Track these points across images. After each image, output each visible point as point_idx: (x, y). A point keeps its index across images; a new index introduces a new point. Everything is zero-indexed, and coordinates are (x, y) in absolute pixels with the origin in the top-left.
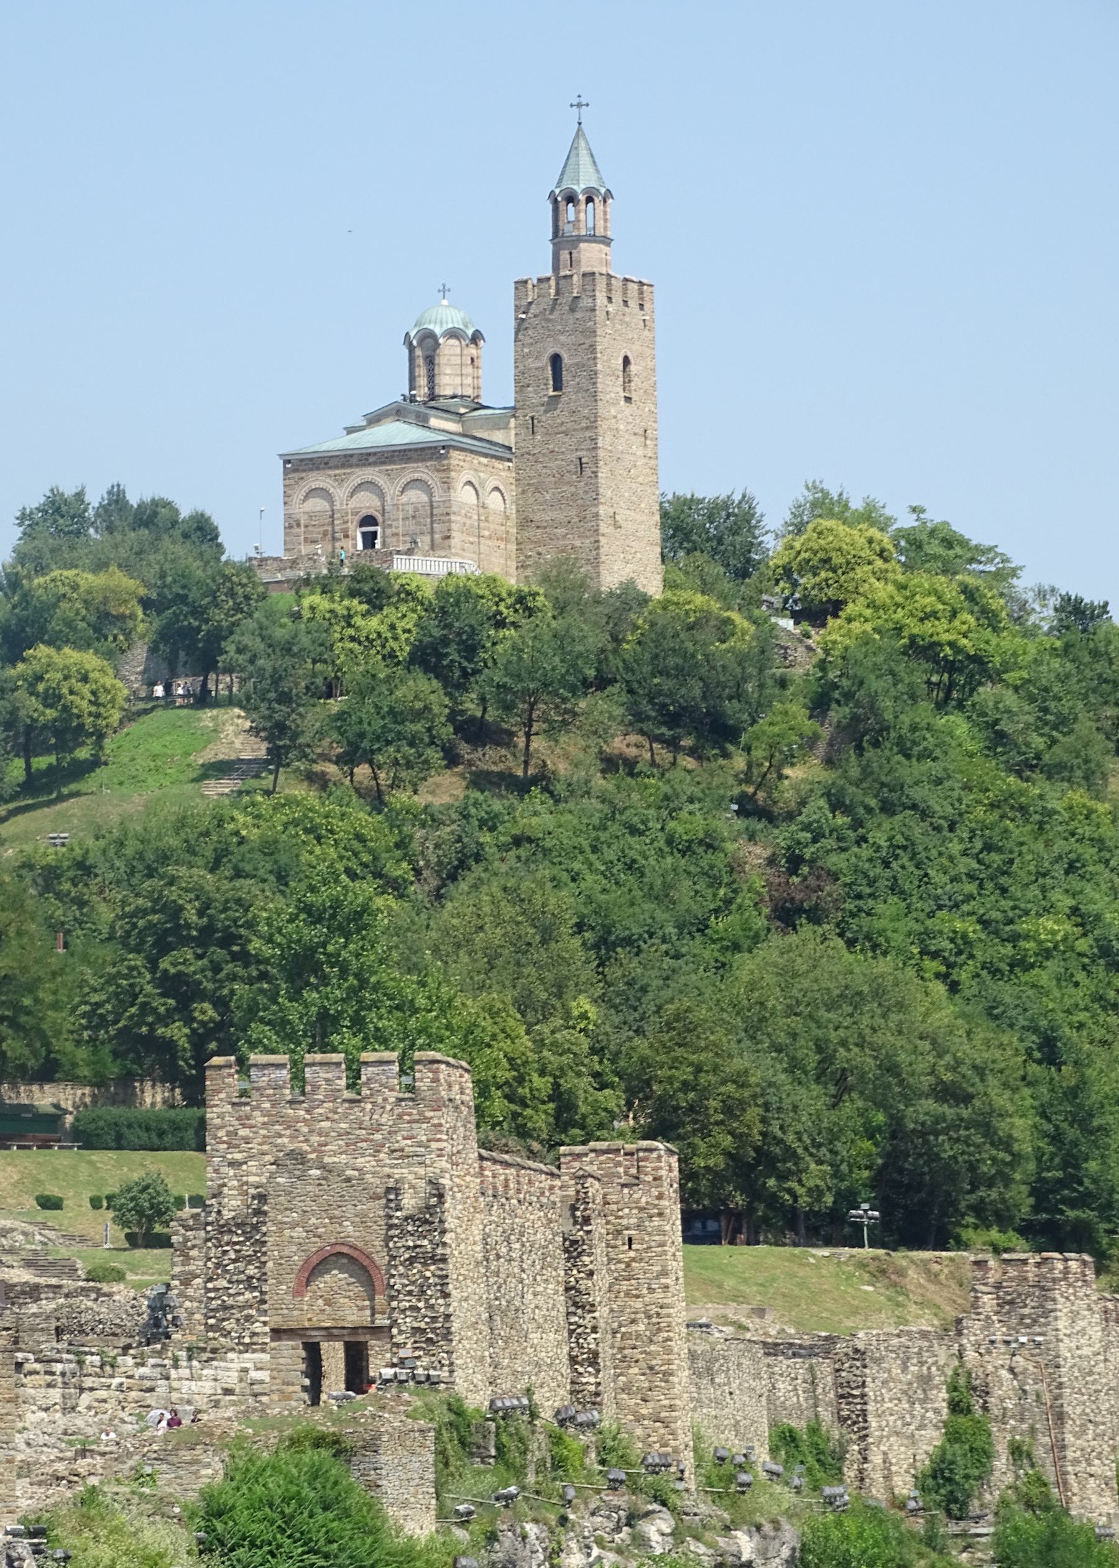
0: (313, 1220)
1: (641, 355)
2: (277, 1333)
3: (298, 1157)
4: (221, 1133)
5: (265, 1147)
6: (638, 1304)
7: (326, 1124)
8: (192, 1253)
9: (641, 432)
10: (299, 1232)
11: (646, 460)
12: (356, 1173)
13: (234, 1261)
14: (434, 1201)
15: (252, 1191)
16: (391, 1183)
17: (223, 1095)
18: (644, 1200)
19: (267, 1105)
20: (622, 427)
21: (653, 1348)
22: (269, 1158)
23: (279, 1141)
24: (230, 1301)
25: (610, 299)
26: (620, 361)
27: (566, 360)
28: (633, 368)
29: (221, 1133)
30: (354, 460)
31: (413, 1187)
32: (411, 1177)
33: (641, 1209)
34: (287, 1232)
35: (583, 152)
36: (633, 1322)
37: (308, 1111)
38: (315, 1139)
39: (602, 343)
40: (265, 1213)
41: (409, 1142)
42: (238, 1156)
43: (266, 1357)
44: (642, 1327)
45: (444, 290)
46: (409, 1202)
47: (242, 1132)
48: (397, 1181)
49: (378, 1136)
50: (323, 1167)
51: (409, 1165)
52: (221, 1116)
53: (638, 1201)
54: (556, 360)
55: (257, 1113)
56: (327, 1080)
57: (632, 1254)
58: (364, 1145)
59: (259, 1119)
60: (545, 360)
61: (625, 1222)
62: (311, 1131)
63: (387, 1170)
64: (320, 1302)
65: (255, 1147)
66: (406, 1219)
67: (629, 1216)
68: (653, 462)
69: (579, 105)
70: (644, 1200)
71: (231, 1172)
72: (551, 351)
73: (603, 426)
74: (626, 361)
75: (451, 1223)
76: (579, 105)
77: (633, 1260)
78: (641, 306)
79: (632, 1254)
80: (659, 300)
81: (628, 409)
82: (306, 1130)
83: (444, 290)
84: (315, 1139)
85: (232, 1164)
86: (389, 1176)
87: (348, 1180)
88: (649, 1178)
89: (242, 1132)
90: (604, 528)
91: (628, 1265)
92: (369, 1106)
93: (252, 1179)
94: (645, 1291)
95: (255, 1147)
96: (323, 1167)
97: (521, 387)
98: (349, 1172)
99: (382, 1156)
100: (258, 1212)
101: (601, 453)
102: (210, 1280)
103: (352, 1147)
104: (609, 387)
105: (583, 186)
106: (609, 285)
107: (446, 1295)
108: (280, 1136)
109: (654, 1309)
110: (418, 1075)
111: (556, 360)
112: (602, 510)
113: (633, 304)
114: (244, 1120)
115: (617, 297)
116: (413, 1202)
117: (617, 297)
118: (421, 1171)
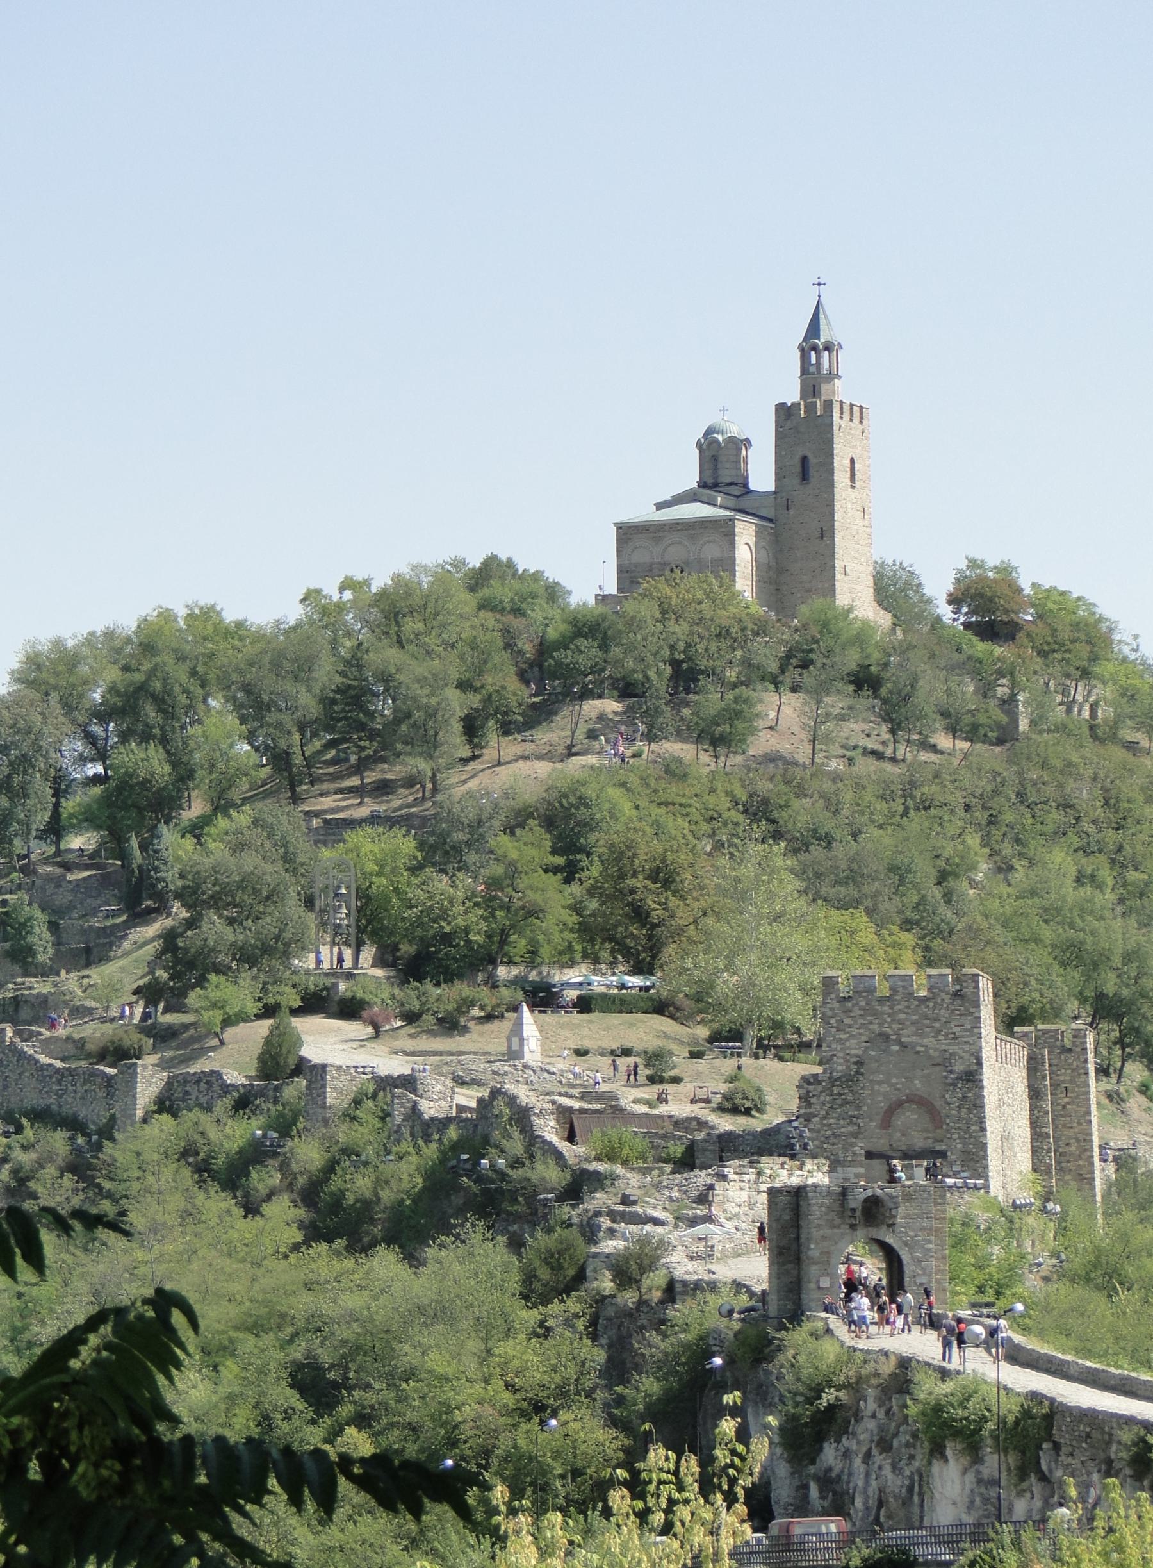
0: (894, 1080)
2: (870, 1155)
3: (885, 1037)
4: (833, 1021)
5: (862, 1031)
6: (1071, 1133)
7: (902, 1016)
8: (813, 1100)
10: (885, 1088)
12: (922, 1049)
13: (841, 1105)
14: (975, 1068)
15: (855, 1060)
16: (947, 1055)
17: (833, 996)
18: (1075, 1063)
19: (863, 1003)
20: (849, 506)
21: (1081, 1163)
22: (864, 1038)
23: (871, 1027)
24: (838, 1132)
25: (841, 418)
26: (848, 461)
27: (813, 460)
28: (857, 466)
29: (833, 1021)
30: (666, 528)
31: (961, 1058)
32: (960, 1052)
33: (1073, 1070)
34: (876, 1087)
35: (822, 316)
36: (1067, 1144)
37: (891, 1007)
38: (896, 1026)
39: (838, 447)
40: (862, 1074)
41: (958, 1029)
42: (843, 1036)
43: (862, 1170)
44: (1073, 1148)
46: (959, 1067)
47: (847, 1021)
48: (951, 1054)
49: (937, 1025)
50: (900, 1043)
51: (958, 1044)
52: (831, 1009)
53: (1072, 1064)
54: (804, 460)
55: (856, 1008)
56: (903, 987)
57: (1067, 1100)
58: (928, 1030)
59: (857, 1012)
61: (1062, 1078)
62: (893, 1021)
63: (944, 1047)
64: (899, 1134)
65: (854, 1031)
66: (957, 1079)
67: (1064, 1074)
68: (868, 530)
69: (819, 284)
70: (1075, 1063)
71: (839, 1047)
74: (852, 461)
75: (985, 1083)
76: (819, 284)
77: (1068, 1103)
78: (861, 422)
79: (1067, 1100)
80: (871, 415)
82: (889, 1020)
83: (724, 410)
84: (896, 1026)
85: (840, 1041)
86: (945, 1051)
87: (918, 1053)
88: (1078, 1049)
89: (847, 1021)
90: (838, 576)
91: (1064, 1107)
92: (931, 1005)
93: (853, 1052)
94: (1075, 1125)
95: (854, 1031)
96: (900, 1043)
97: (780, 476)
98: (919, 1049)
99: (941, 1038)
100: (858, 1073)
101: (836, 523)
102: (824, 1118)
103: (919, 1032)
104: (841, 478)
105: (822, 340)
106: (841, 408)
107: (983, 1130)
108: (871, 1023)
109: (1081, 1137)
110: (964, 984)
111: (804, 460)
112: (838, 564)
113: (856, 419)
114: (847, 1011)
115: (846, 416)
116: (961, 1068)
117: (846, 416)
118: (967, 1047)
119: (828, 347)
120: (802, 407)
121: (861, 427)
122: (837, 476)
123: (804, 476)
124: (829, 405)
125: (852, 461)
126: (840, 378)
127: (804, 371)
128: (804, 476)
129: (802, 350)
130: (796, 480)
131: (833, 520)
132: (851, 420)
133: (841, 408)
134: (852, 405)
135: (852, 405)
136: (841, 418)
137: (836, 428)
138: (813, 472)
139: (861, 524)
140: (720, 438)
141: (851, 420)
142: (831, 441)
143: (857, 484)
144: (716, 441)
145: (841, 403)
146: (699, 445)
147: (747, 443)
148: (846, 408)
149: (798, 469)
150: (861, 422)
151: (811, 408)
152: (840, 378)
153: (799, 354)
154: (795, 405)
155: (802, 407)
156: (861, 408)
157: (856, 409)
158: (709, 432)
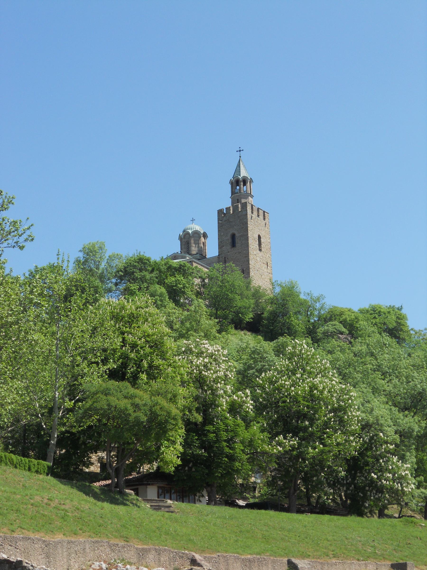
1: (264, 236)
9: (266, 263)
11: (268, 274)
20: (258, 259)
25: (252, 213)
27: (237, 235)
28: (262, 240)
35: (242, 166)
45: (193, 220)
54: (233, 236)
60: (229, 237)
68: (270, 275)
72: (231, 232)
73: (251, 257)
74: (259, 237)
76: (240, 151)
78: (264, 219)
81: (261, 254)
83: (193, 220)
104: (253, 244)
105: (241, 176)
106: (252, 208)
111: (233, 236)
113: (261, 217)
115: (255, 213)
119: (245, 181)
120: (231, 209)
121: (264, 222)
122: (251, 241)
123: (233, 244)
124: (244, 206)
125: (259, 237)
126: (252, 196)
127: (233, 193)
128: (233, 244)
129: (231, 183)
130: (229, 247)
131: (249, 264)
132: (258, 216)
133: (252, 208)
134: (258, 209)
135: (258, 209)
136: (252, 213)
137: (249, 217)
138: (237, 241)
139: (265, 270)
140: (190, 232)
141: (258, 216)
142: (247, 223)
143: (262, 249)
144: (188, 233)
145: (252, 206)
146: (181, 238)
147: (205, 235)
148: (255, 209)
149: (230, 241)
150: (264, 219)
151: (235, 208)
152: (252, 196)
153: (230, 186)
154: (228, 209)
155: (231, 209)
156: (264, 212)
157: (261, 212)
158: (184, 231)
